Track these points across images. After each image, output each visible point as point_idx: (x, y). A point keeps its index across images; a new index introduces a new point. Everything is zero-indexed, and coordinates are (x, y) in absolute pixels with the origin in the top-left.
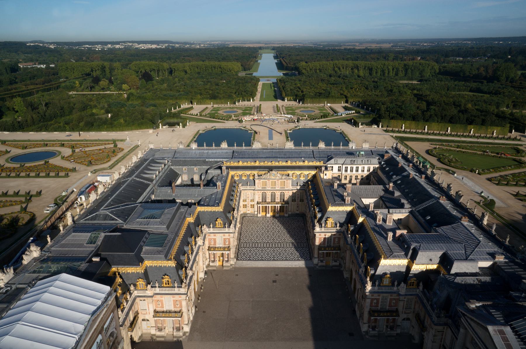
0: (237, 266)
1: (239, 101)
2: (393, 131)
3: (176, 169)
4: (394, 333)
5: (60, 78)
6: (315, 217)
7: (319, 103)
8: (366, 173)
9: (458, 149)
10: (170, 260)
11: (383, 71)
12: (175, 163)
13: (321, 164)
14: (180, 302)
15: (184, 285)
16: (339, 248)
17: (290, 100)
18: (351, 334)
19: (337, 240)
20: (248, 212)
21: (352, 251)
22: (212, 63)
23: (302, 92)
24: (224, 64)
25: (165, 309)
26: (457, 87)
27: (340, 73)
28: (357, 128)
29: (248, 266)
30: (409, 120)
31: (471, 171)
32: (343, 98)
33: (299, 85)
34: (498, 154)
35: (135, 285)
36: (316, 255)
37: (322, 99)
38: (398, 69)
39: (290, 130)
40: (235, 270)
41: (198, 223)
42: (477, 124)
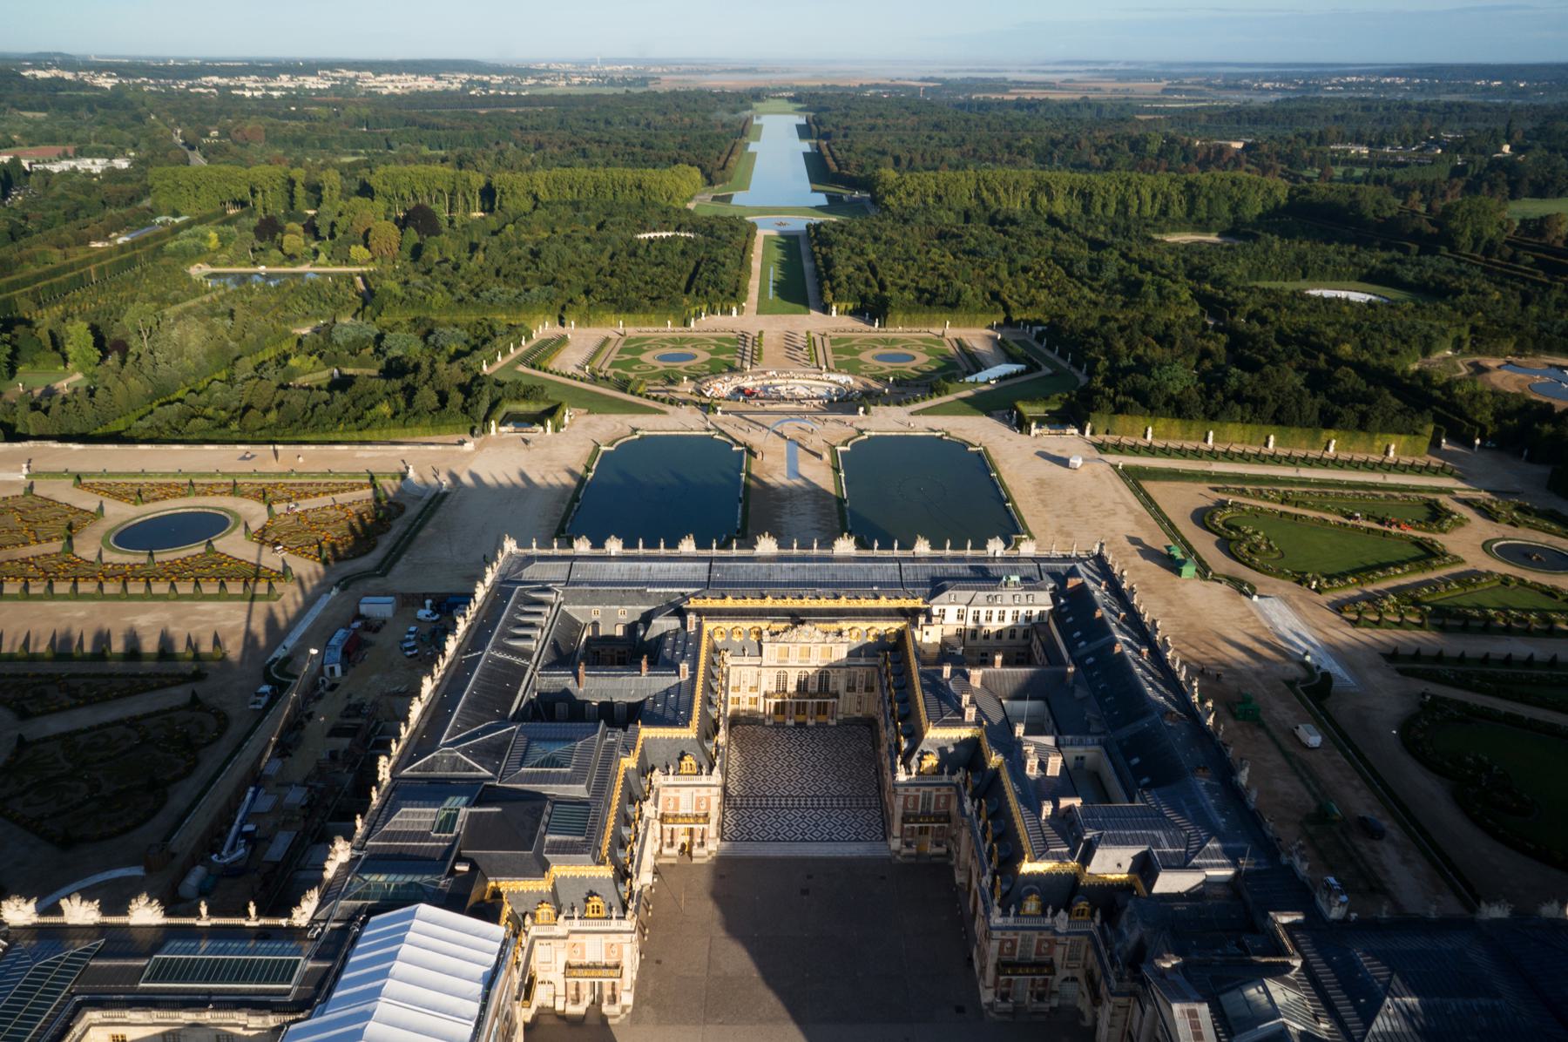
2: (1119, 449)
4: (1045, 1006)
6: (898, 750)
7: (930, 323)
9: (1281, 508)
11: (1123, 203)
13: (919, 603)
14: (620, 947)
15: (629, 914)
16: (948, 818)
18: (960, 1010)
19: (942, 801)
21: (973, 832)
23: (882, 287)
25: (587, 961)
26: (1330, 268)
27: (995, 207)
28: (1025, 437)
30: (1166, 416)
31: (1300, 582)
32: (996, 311)
33: (873, 256)
34: (1381, 522)
36: (896, 832)
38: (1167, 197)
39: (845, 444)
41: (645, 770)
42: (1345, 428)
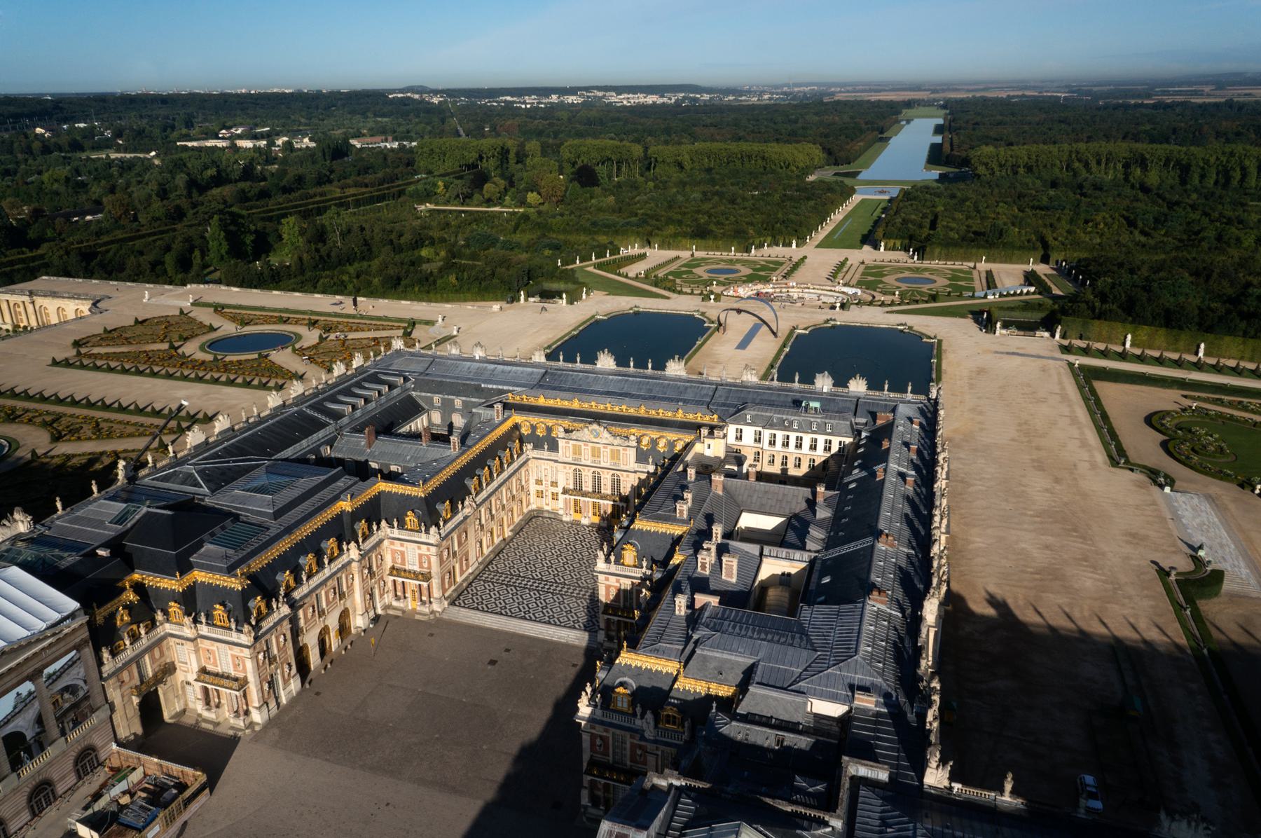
0: (445, 616)
1: (761, 246)
3: (420, 397)
5: (416, 173)
8: (820, 455)
10: (235, 576)
11: (1225, 173)
12: (420, 386)
17: (894, 249)
20: (546, 508)
22: (745, 146)
24: (773, 149)
28: (990, 336)
29: (464, 621)
30: (1151, 324)
32: (1035, 248)
35: (166, 613)
37: (974, 251)
40: (437, 625)
